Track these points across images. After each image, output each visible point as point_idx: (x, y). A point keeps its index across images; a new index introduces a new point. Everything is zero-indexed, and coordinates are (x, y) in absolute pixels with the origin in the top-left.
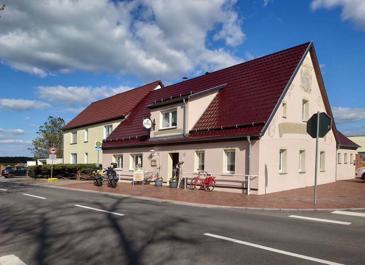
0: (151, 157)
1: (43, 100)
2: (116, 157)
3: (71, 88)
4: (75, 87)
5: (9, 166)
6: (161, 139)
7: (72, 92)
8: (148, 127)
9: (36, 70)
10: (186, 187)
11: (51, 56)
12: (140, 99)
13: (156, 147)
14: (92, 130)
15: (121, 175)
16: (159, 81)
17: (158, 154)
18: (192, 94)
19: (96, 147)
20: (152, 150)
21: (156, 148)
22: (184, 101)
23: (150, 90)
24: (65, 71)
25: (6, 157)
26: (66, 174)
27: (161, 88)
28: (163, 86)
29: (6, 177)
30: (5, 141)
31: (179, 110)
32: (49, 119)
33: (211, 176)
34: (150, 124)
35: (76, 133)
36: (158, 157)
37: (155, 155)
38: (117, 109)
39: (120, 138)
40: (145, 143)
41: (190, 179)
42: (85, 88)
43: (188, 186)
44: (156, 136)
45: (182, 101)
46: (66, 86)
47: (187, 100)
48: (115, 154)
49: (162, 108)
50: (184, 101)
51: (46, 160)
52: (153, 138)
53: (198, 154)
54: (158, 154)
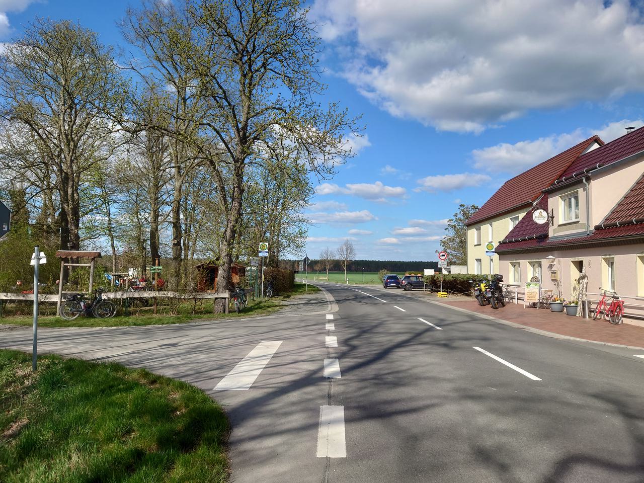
0: (551, 266)
1: (478, 171)
2: (534, 265)
3: (520, 144)
4: (526, 142)
5: (407, 275)
6: (560, 239)
7: (521, 150)
8: (541, 221)
9: (469, 126)
10: (589, 315)
11: (490, 97)
12: (558, 173)
13: (556, 252)
14: (497, 224)
15: (518, 293)
16: (594, 137)
17: (559, 262)
18: (599, 167)
19: (487, 252)
20: (551, 257)
21: (556, 253)
22: (584, 180)
23: (577, 155)
24: (512, 115)
25: (377, 260)
26: (458, 288)
27: (599, 146)
28: (603, 143)
29: (405, 290)
30: (430, 238)
31: (581, 190)
32: (459, 208)
33: (620, 299)
34: (545, 217)
35: (480, 229)
36: (559, 266)
37: (555, 263)
38: (529, 191)
39: (531, 236)
40: (542, 245)
41: (594, 303)
42: (544, 141)
43: (593, 314)
44: (556, 235)
45: (581, 181)
46: (513, 143)
47: (588, 179)
48: (532, 261)
49: (561, 192)
50: (584, 180)
51: (450, 268)
52: (552, 238)
53: (607, 260)
54: (559, 262)
